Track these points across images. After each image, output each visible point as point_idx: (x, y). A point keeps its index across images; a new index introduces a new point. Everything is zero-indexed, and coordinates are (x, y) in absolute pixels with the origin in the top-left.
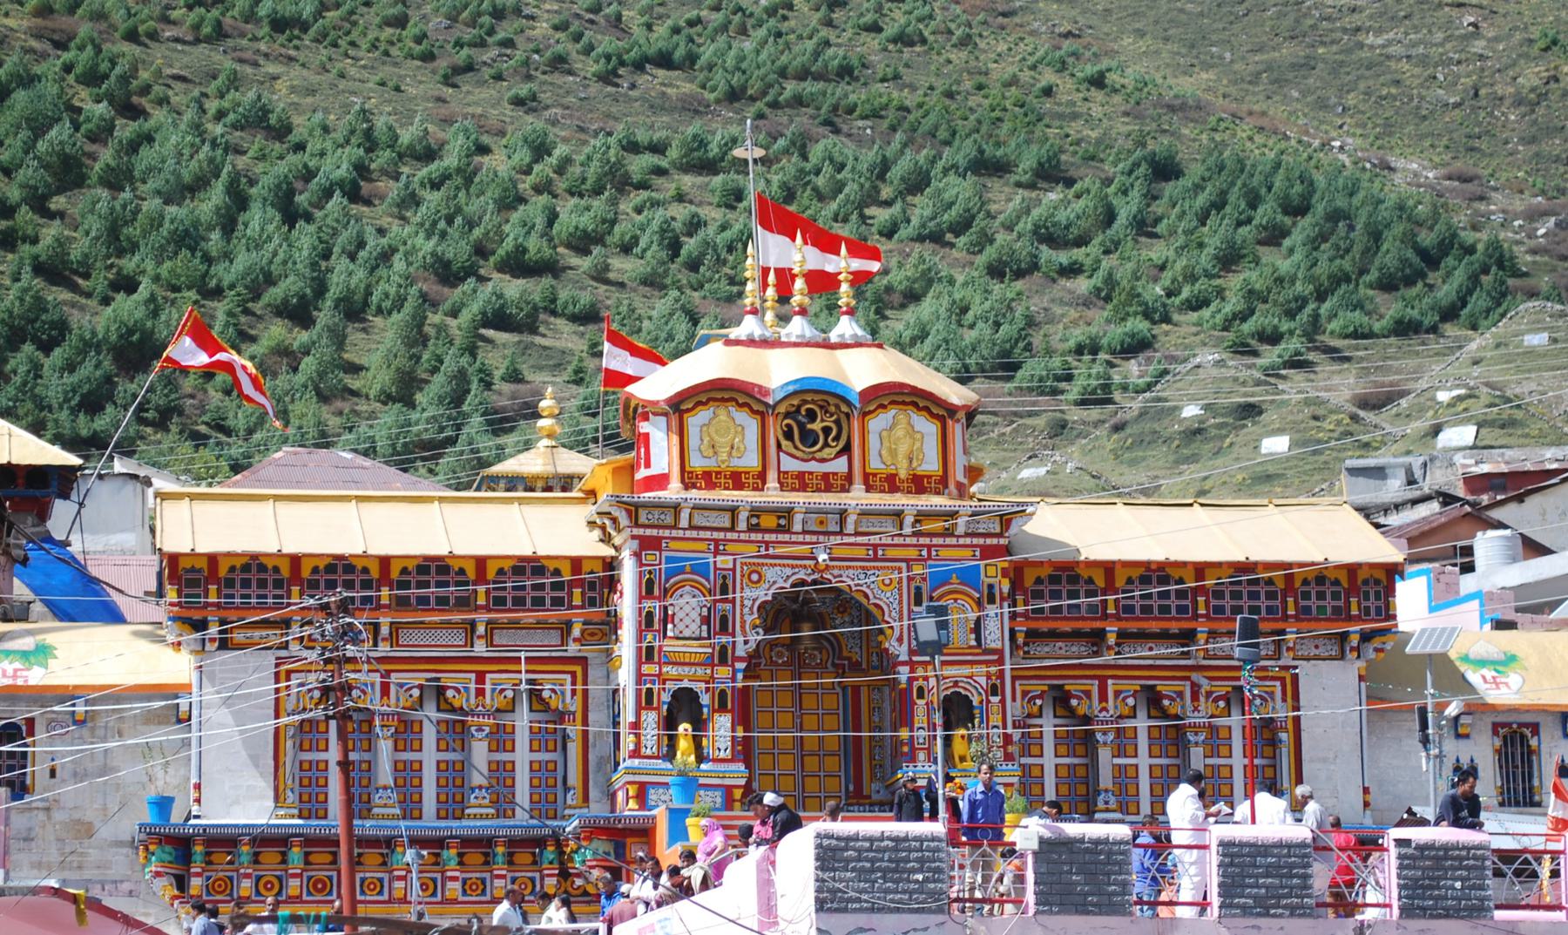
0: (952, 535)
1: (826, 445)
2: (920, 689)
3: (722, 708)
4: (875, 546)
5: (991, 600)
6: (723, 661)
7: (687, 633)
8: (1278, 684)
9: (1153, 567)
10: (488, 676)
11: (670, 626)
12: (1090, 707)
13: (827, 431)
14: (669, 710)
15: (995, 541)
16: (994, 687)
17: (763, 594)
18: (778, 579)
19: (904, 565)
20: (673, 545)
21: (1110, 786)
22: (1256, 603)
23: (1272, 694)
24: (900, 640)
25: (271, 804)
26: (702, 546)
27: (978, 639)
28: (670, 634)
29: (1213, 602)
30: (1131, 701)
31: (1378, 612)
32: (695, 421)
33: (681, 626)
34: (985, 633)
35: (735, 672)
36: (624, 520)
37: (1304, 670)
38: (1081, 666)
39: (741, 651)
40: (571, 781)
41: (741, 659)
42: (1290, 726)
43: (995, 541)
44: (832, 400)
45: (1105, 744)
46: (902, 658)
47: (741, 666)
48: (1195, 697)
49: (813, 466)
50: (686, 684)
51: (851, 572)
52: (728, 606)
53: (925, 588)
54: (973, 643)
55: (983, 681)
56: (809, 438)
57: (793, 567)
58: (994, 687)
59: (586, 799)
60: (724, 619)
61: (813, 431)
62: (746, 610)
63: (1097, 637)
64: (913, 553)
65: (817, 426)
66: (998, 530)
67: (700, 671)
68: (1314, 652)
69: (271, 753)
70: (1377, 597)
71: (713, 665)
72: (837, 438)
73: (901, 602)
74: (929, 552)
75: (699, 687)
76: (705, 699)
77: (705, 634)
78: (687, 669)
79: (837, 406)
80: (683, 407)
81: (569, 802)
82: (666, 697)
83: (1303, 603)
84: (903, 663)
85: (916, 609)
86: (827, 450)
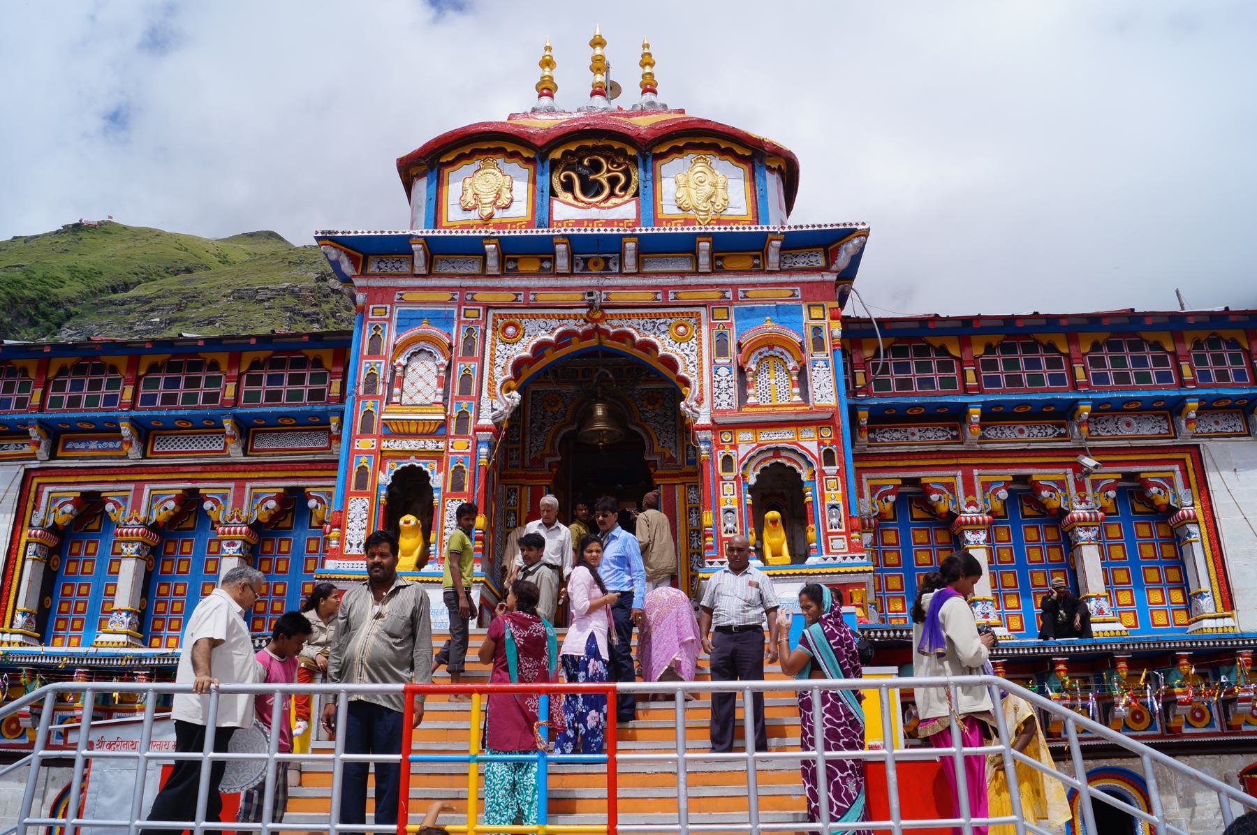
0: (763, 271)
1: (612, 194)
2: (727, 460)
4: (664, 289)
5: (819, 345)
6: (462, 430)
7: (419, 399)
8: (1177, 468)
9: (1020, 324)
10: (248, 485)
11: (397, 390)
12: (954, 502)
13: (613, 181)
14: (387, 499)
15: (816, 277)
17: (522, 349)
18: (541, 332)
19: (703, 311)
20: (408, 296)
23: (1170, 481)
24: (700, 401)
26: (446, 296)
27: (804, 394)
28: (395, 399)
29: (1092, 370)
34: (813, 387)
36: (347, 268)
37: (1212, 449)
39: (486, 420)
41: (482, 429)
42: (1200, 517)
43: (816, 277)
44: (617, 145)
48: (1080, 486)
49: (593, 213)
50: (413, 461)
51: (635, 321)
52: (474, 365)
54: (797, 398)
55: (813, 447)
56: (591, 188)
60: (466, 378)
61: (596, 181)
62: (497, 371)
63: (957, 416)
64: (714, 295)
65: (603, 177)
67: (430, 445)
68: (1214, 428)
71: (446, 437)
72: (625, 188)
73: (700, 355)
74: (735, 295)
75: (428, 467)
76: (436, 480)
77: (440, 399)
78: (413, 442)
79: (622, 152)
80: (443, 160)
82: (385, 478)
83: (1198, 368)
86: (614, 200)
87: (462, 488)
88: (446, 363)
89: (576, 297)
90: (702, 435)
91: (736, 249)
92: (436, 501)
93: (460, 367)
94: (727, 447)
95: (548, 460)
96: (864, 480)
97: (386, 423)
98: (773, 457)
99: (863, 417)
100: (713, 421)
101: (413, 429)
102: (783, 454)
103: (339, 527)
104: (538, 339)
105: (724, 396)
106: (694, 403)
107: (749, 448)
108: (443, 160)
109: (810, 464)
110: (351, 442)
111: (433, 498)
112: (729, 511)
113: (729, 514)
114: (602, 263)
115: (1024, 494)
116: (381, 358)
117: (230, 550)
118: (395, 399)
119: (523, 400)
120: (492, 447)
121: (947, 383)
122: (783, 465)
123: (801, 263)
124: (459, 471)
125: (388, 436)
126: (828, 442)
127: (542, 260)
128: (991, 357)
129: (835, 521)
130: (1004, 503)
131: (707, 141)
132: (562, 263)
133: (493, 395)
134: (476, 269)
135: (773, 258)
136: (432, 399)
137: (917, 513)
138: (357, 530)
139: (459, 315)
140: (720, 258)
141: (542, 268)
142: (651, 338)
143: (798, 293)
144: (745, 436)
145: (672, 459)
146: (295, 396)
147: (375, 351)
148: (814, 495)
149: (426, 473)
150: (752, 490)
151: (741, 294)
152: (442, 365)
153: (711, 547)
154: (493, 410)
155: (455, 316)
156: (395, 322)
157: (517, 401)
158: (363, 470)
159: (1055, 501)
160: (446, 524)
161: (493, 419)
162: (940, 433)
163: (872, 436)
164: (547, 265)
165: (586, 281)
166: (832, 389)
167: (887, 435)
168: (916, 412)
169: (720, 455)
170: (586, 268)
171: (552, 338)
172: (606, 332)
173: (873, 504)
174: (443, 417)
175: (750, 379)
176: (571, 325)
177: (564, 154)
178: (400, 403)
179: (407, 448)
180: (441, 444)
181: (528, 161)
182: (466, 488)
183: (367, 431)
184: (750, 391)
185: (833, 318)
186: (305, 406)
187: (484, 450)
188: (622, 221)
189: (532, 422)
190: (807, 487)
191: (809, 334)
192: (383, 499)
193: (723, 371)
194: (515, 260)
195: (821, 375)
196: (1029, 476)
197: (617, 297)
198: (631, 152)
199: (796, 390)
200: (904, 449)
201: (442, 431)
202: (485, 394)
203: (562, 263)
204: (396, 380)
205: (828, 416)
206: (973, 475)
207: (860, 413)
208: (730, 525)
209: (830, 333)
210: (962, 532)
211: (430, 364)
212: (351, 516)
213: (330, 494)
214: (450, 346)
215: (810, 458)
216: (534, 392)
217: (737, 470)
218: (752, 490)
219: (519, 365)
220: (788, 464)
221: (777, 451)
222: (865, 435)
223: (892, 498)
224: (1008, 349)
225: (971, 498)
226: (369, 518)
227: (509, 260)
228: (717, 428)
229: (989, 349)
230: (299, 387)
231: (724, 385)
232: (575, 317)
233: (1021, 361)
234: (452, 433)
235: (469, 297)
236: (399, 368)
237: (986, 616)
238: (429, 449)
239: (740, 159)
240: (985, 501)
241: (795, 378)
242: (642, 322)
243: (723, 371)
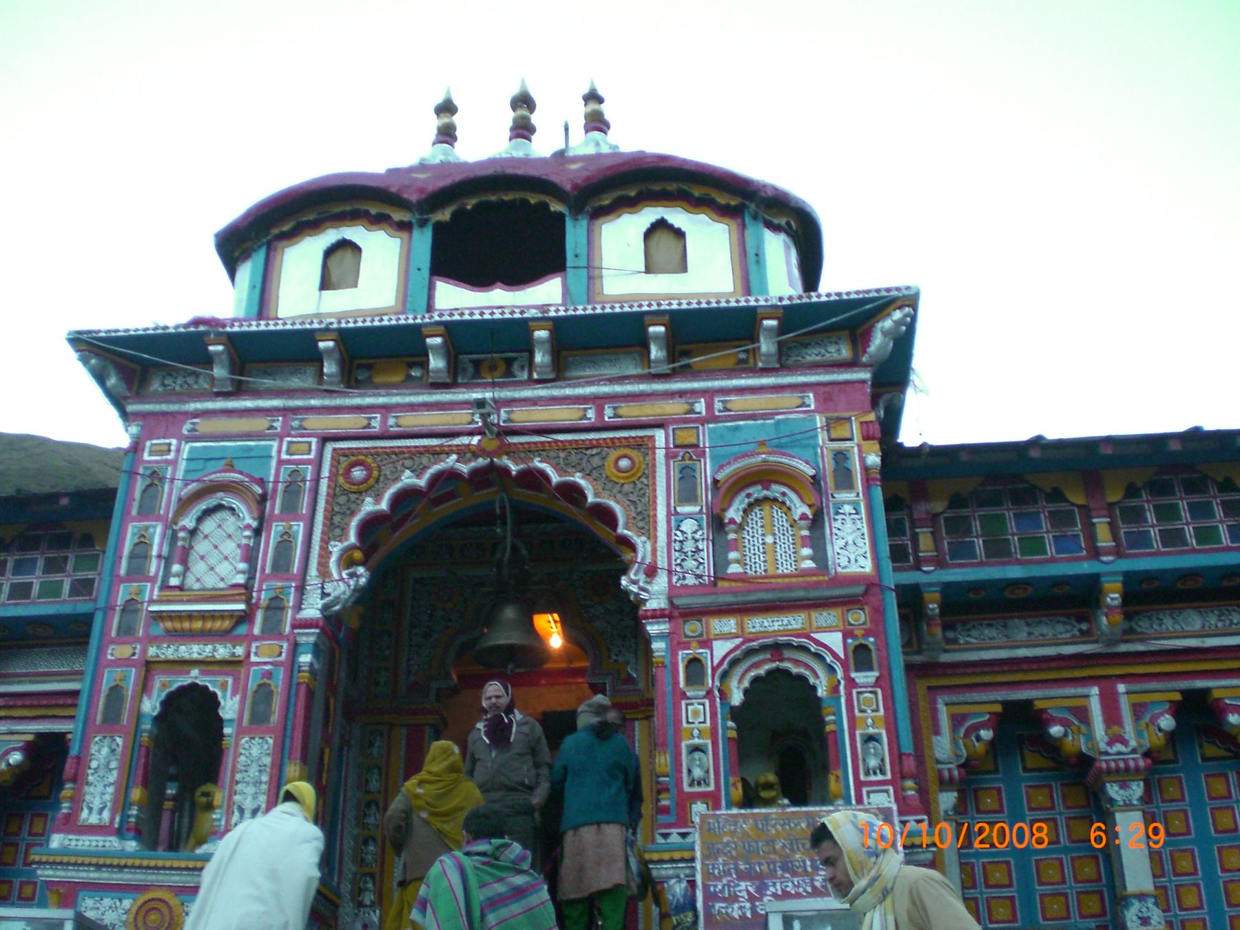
2: (695, 664)
3: (257, 720)
5: (844, 481)
6: (273, 630)
7: (210, 581)
9: (1175, 446)
11: (176, 568)
12: (1090, 737)
16: (861, 649)
19: (660, 436)
20: (204, 425)
24: (651, 571)
26: (260, 424)
30: (1167, 722)
33: (198, 568)
35: (295, 648)
38: (1060, 658)
39: (312, 611)
45: (1128, 806)
46: (652, 605)
47: (309, 637)
50: (195, 676)
51: (552, 454)
53: (707, 470)
55: (834, 640)
57: (437, 453)
58: (861, 649)
64: (674, 408)
66: (845, 353)
74: (710, 406)
76: (229, 707)
78: (196, 648)
82: (151, 706)
84: (657, 615)
87: (267, 719)
88: (255, 524)
89: (461, 418)
90: (653, 629)
91: (705, 335)
92: (228, 742)
93: (277, 528)
94: (694, 644)
95: (435, 685)
96: (942, 708)
97: (159, 616)
98: (772, 661)
100: (671, 603)
101: (198, 625)
102: (787, 654)
103: (74, 780)
104: (399, 485)
105: (690, 564)
106: (642, 577)
107: (729, 645)
108: (275, 231)
109: (831, 669)
110: (102, 649)
111: (221, 736)
112: (696, 749)
113: (697, 755)
114: (502, 367)
116: (158, 518)
118: (174, 581)
119: (370, 582)
120: (316, 650)
122: (786, 672)
123: (812, 356)
124: (264, 692)
125: (154, 640)
126: (859, 633)
127: (411, 366)
128: (1134, 502)
129: (873, 763)
130: (1171, 737)
131: (672, 187)
132: (436, 363)
133: (324, 573)
134: (309, 383)
135: (766, 346)
137: (1033, 760)
138: (100, 788)
139: (279, 451)
140: (688, 354)
141: (409, 377)
142: (578, 478)
143: (811, 398)
145: (630, 680)
146: (51, 591)
148: (839, 722)
149: (215, 694)
150: (735, 713)
151: (718, 405)
152: (248, 527)
153: (665, 810)
154: (324, 595)
155: (274, 453)
156: (183, 465)
157: (363, 581)
158: (116, 692)
160: (238, 777)
161: (325, 608)
162: (1060, 628)
163: (950, 635)
164: (416, 373)
165: (476, 395)
166: (867, 548)
167: (975, 633)
168: (1020, 594)
169: (682, 655)
170: (477, 374)
171: (422, 482)
172: (506, 471)
173: (954, 741)
174: (242, 607)
175: (732, 536)
177: (454, 215)
178: (180, 588)
179: (187, 656)
180: (240, 651)
181: (404, 227)
182: (275, 718)
183: (127, 632)
184: (733, 555)
185: (867, 437)
186: (64, 605)
187: (306, 658)
189: (413, 626)
190: (827, 707)
191: (829, 465)
192: (145, 737)
193: (688, 526)
194: (369, 367)
195: (849, 526)
196: (1207, 691)
197: (522, 416)
198: (556, 207)
199: (807, 551)
200: (1003, 654)
201: (242, 630)
202: (313, 571)
203: (436, 363)
205: (860, 589)
206: (1117, 693)
207: (927, 596)
208: (698, 773)
209: (862, 460)
210: (1103, 790)
211: (230, 523)
212: (94, 764)
214: (263, 498)
215: (829, 659)
216: (416, 581)
218: (735, 713)
219: (370, 526)
220: (795, 670)
221: (776, 649)
222: (938, 631)
223: (986, 734)
224: (1160, 488)
225: (1115, 729)
226: (120, 768)
227: (360, 366)
228: (675, 613)
229: (1132, 491)
230: (56, 577)
231: (689, 547)
232: (462, 452)
233: (1183, 505)
234: (257, 630)
235: (296, 424)
236: (182, 534)
238: (218, 657)
239: (723, 212)
240: (1139, 734)
241: (805, 533)
242: (562, 455)
243: (688, 526)
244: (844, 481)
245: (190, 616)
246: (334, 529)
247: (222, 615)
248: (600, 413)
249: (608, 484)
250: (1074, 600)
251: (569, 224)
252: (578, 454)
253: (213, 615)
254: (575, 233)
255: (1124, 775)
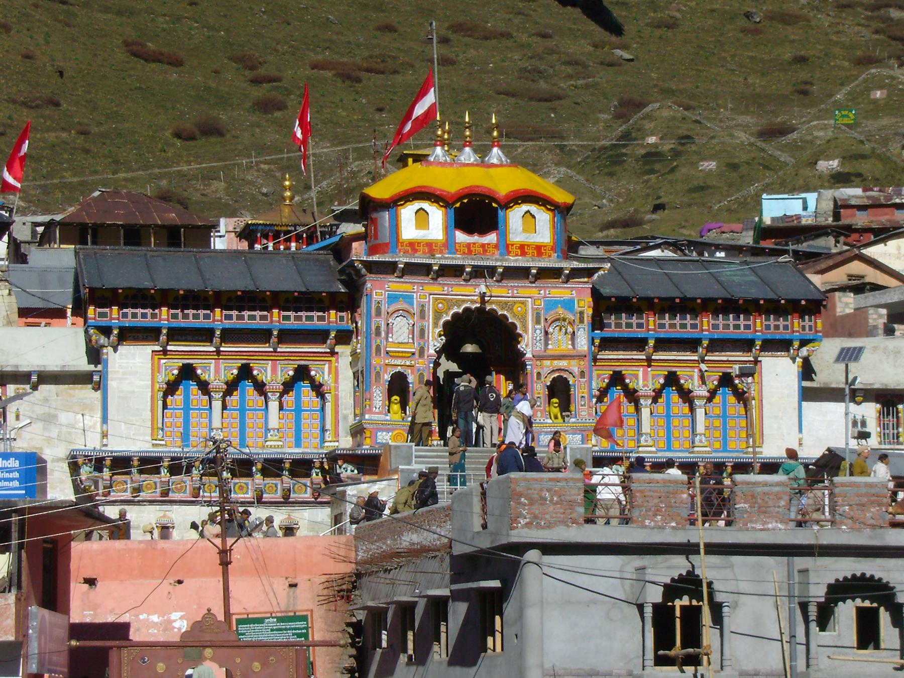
2: (539, 374)
12: (638, 384)
19: (530, 300)
21: (649, 431)
22: (738, 322)
25: (150, 438)
27: (573, 344)
28: (390, 340)
29: (712, 322)
31: (810, 329)
32: (407, 212)
40: (328, 426)
45: (646, 406)
50: (399, 369)
54: (570, 347)
57: (464, 301)
59: (337, 434)
69: (149, 408)
70: (810, 320)
75: (408, 372)
76: (410, 379)
77: (411, 341)
81: (327, 439)
82: (387, 377)
84: (530, 359)
85: (538, 327)
99: (597, 342)
115: (672, 380)
117: (273, 398)
121: (640, 326)
136: (406, 341)
142: (505, 313)
144: (547, 363)
147: (378, 313)
159: (688, 385)
161: (435, 350)
176: (468, 305)
188: (489, 244)
193: (538, 332)
202: (431, 338)
204: (389, 330)
213: (323, 369)
217: (543, 379)
219: (446, 324)
237: (646, 441)
243: (538, 332)
244: (582, 321)
245: (399, 352)
246: (436, 325)
247: (408, 352)
248: (513, 292)
249: (515, 316)
250: (639, 344)
251: (500, 211)
252: (505, 305)
253: (405, 352)
254: (501, 213)
255: (646, 397)
